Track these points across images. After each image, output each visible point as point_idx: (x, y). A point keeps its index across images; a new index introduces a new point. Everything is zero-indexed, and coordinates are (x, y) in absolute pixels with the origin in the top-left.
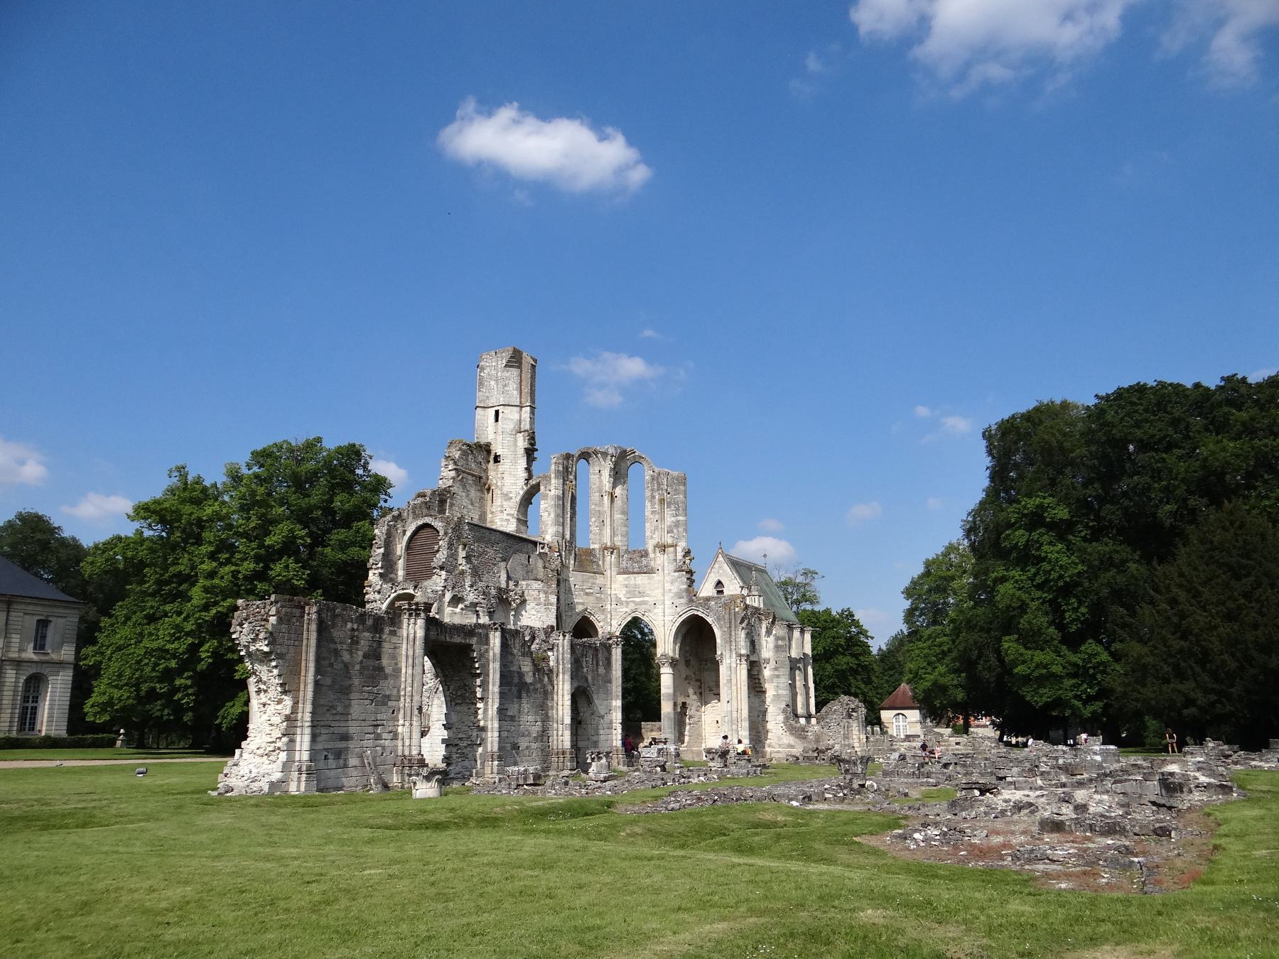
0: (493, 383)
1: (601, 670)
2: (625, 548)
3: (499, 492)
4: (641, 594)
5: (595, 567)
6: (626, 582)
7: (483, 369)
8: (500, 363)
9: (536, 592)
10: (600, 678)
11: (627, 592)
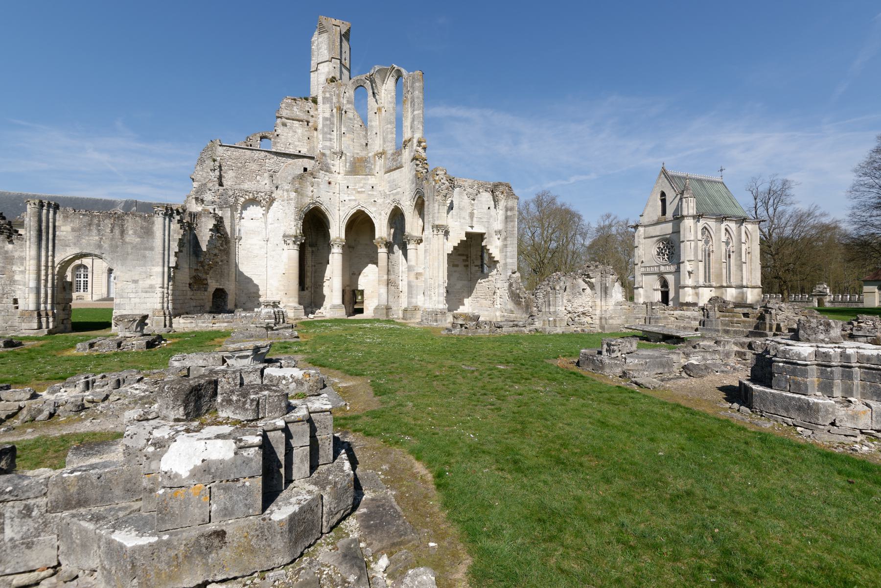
1: (131, 237)
7: (314, 43)
9: (281, 192)
10: (129, 247)
11: (390, 187)
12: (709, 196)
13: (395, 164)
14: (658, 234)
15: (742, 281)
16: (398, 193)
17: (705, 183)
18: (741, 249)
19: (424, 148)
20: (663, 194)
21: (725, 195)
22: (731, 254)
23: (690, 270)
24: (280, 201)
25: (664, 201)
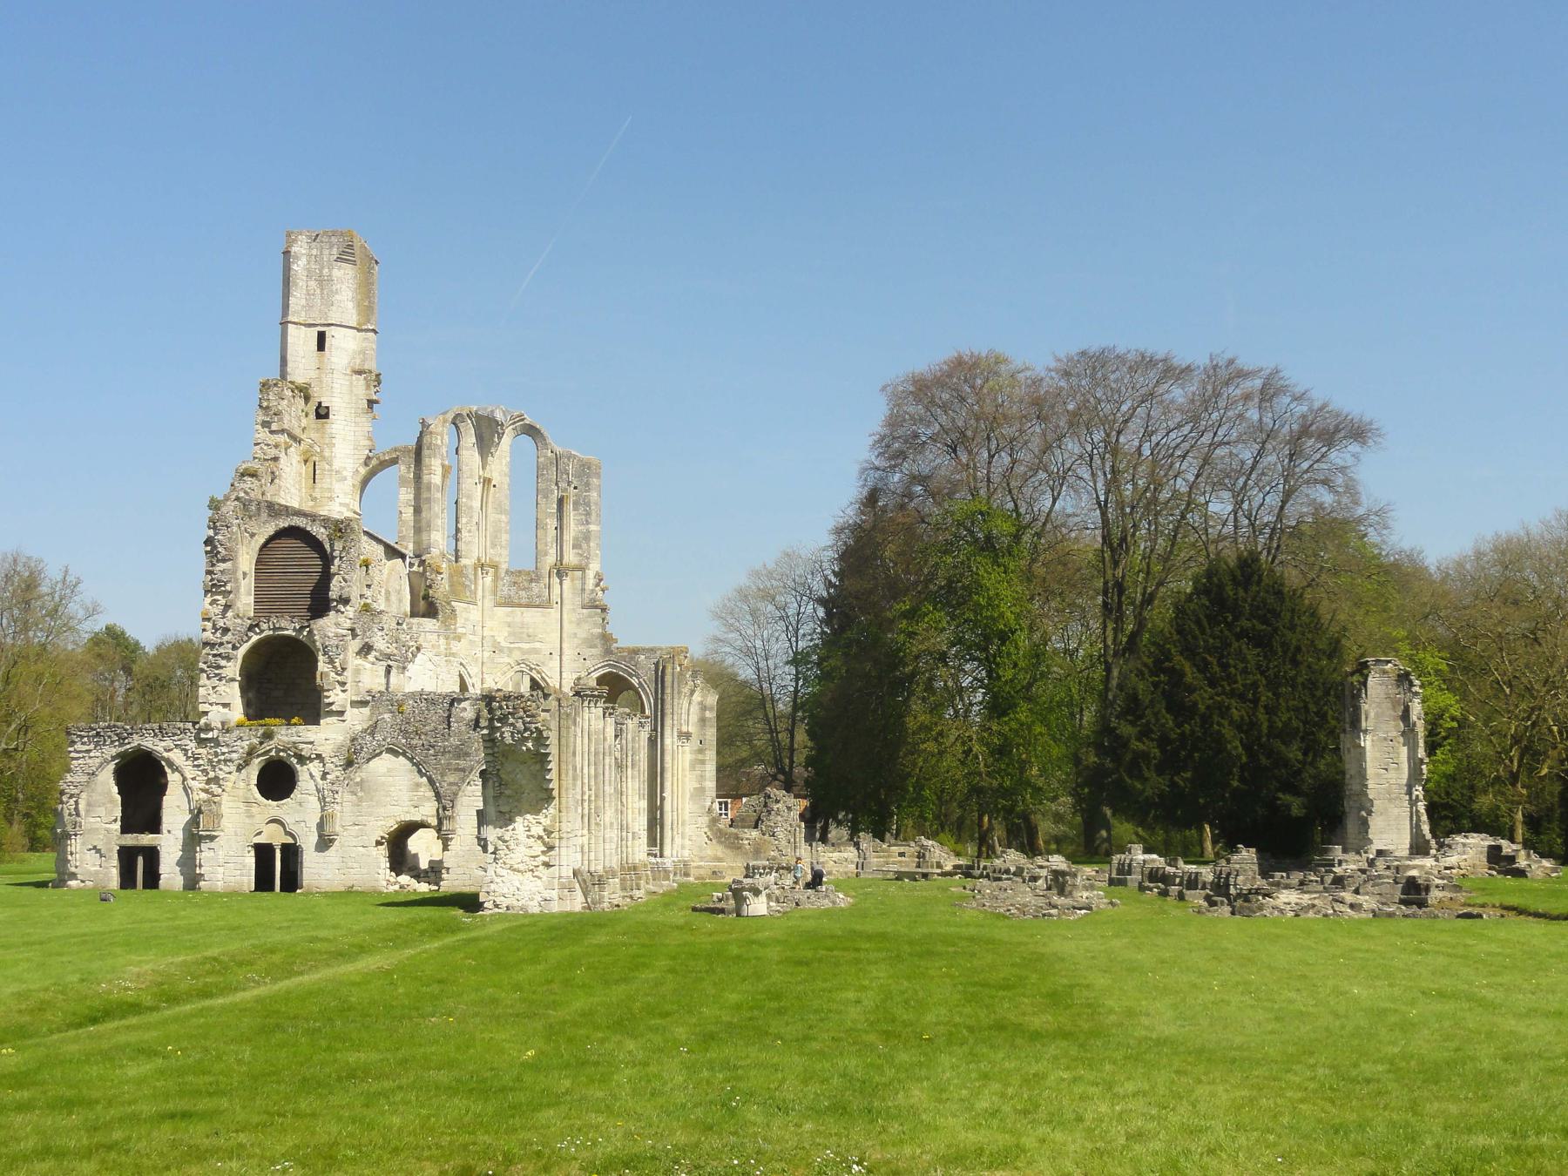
0: (313, 284)
2: (504, 567)
3: (327, 467)
4: (531, 637)
5: (468, 594)
6: (509, 619)
8: (326, 252)
11: (510, 634)
13: (523, 593)
16: (536, 651)
19: (603, 590)
24: (431, 655)
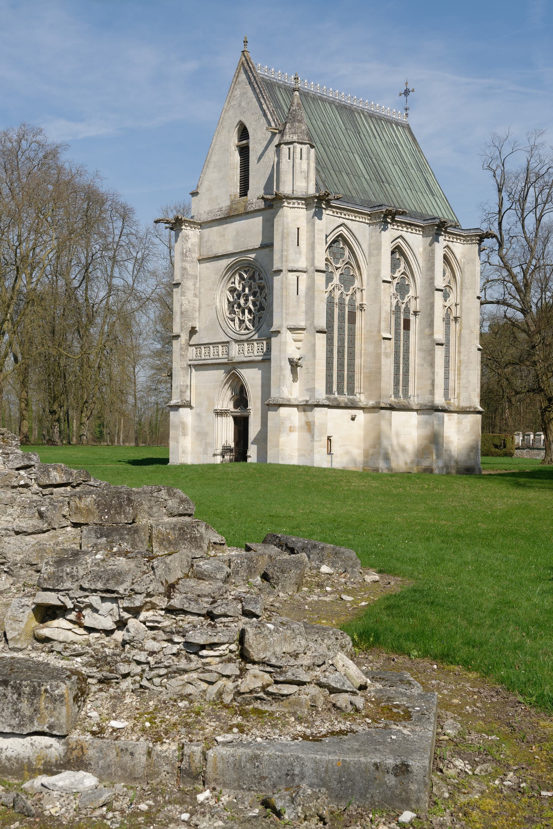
12: (366, 154)
14: (230, 249)
15: (432, 393)
17: (361, 121)
18: (432, 306)
20: (244, 133)
21: (409, 159)
22: (412, 318)
23: (296, 356)
25: (244, 151)
